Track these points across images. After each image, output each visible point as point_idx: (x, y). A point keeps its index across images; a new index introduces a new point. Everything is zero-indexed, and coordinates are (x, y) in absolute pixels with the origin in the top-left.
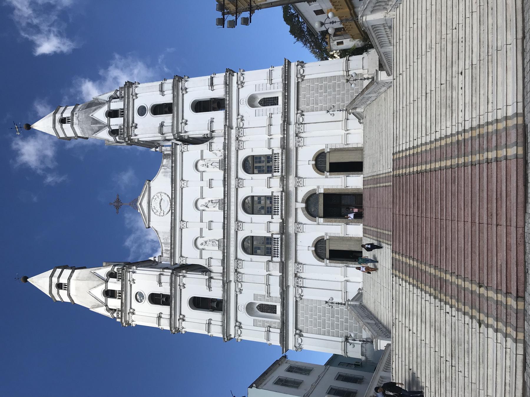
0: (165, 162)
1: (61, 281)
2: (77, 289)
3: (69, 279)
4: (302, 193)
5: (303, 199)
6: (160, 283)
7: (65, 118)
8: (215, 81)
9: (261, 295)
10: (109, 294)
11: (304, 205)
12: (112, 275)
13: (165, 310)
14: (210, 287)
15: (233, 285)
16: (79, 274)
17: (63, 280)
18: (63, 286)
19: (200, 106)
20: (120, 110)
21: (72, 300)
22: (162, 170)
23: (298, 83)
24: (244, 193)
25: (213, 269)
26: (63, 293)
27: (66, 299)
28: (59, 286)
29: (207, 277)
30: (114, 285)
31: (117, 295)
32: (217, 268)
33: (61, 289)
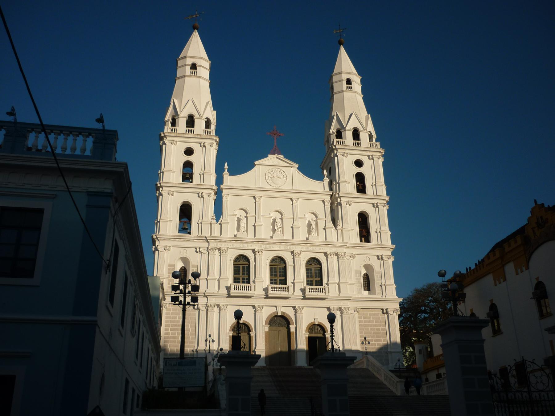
1: (198, 68)
3: (200, 77)
4: (290, 313)
7: (351, 84)
10: (191, 122)
11: (279, 314)
12: (208, 124)
15: (206, 245)
18: (193, 71)
19: (363, 219)
20: (359, 142)
21: (179, 78)
23: (382, 310)
24: (288, 257)
27: (179, 73)
28: (194, 66)
30: (199, 125)
31: (190, 129)
33: (191, 68)
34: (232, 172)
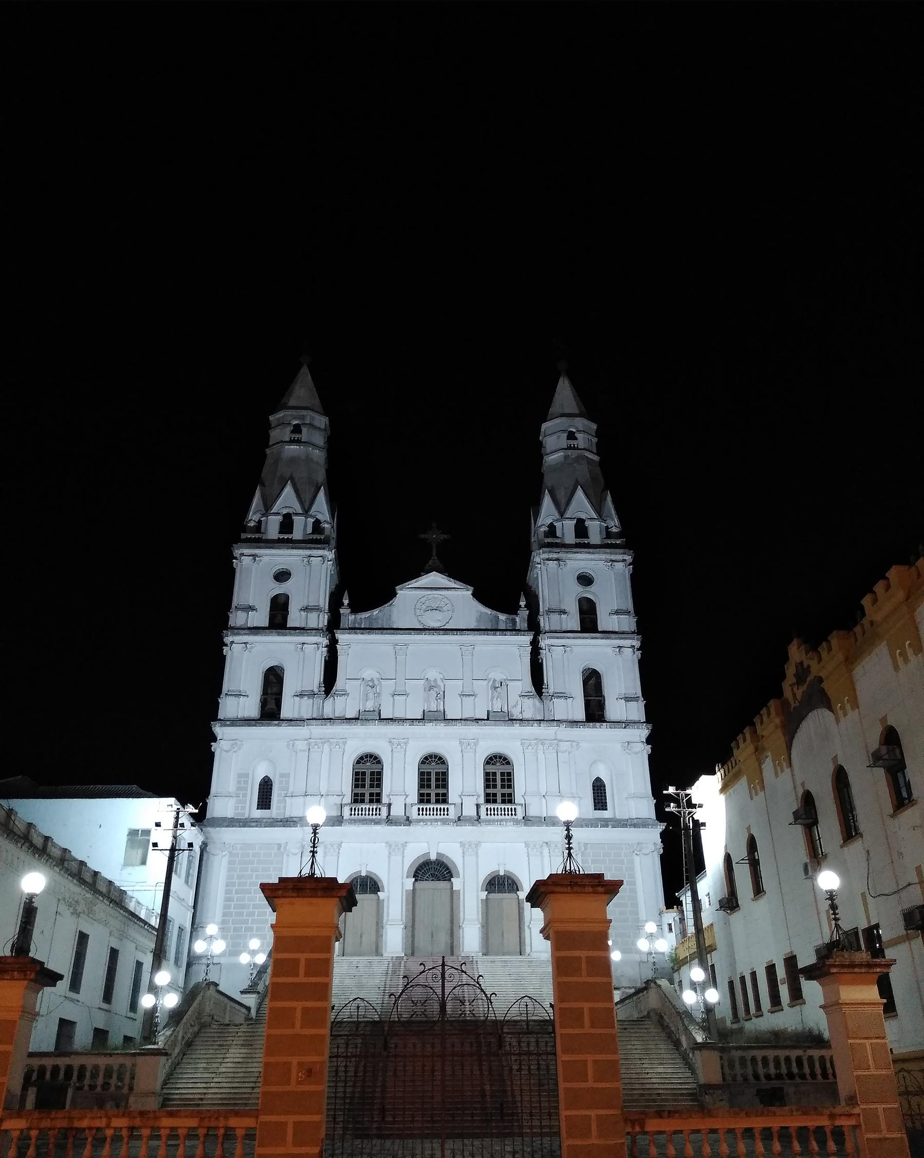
0: (502, 617)
2: (293, 460)
5: (443, 855)
6: (306, 609)
8: (633, 704)
9: (287, 783)
13: (261, 618)
14: (301, 695)
16: (318, 463)
17: (305, 435)
22: (488, 611)
25: (329, 702)
26: (286, 434)
29: (316, 690)
32: (332, 706)
34: (356, 608)
